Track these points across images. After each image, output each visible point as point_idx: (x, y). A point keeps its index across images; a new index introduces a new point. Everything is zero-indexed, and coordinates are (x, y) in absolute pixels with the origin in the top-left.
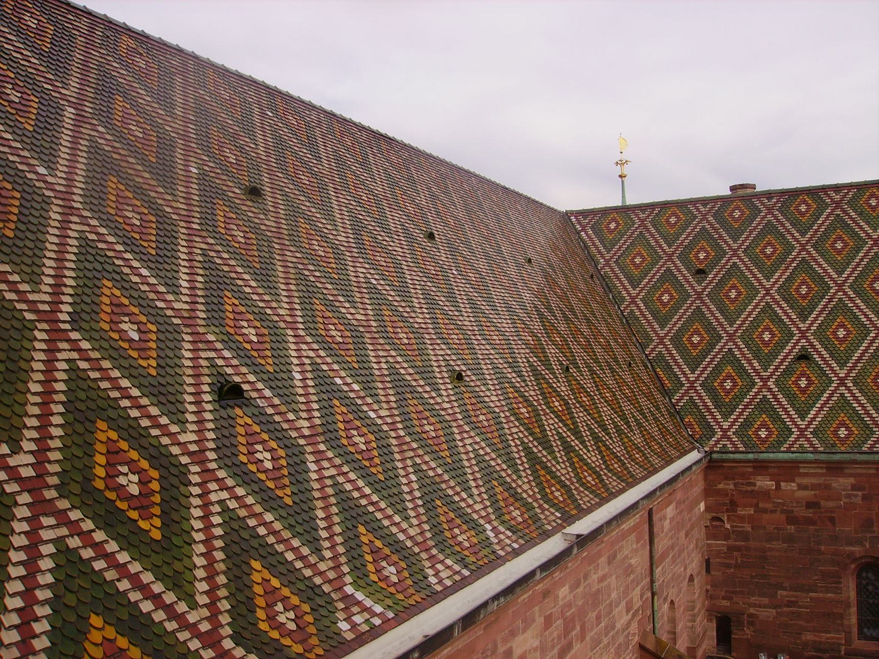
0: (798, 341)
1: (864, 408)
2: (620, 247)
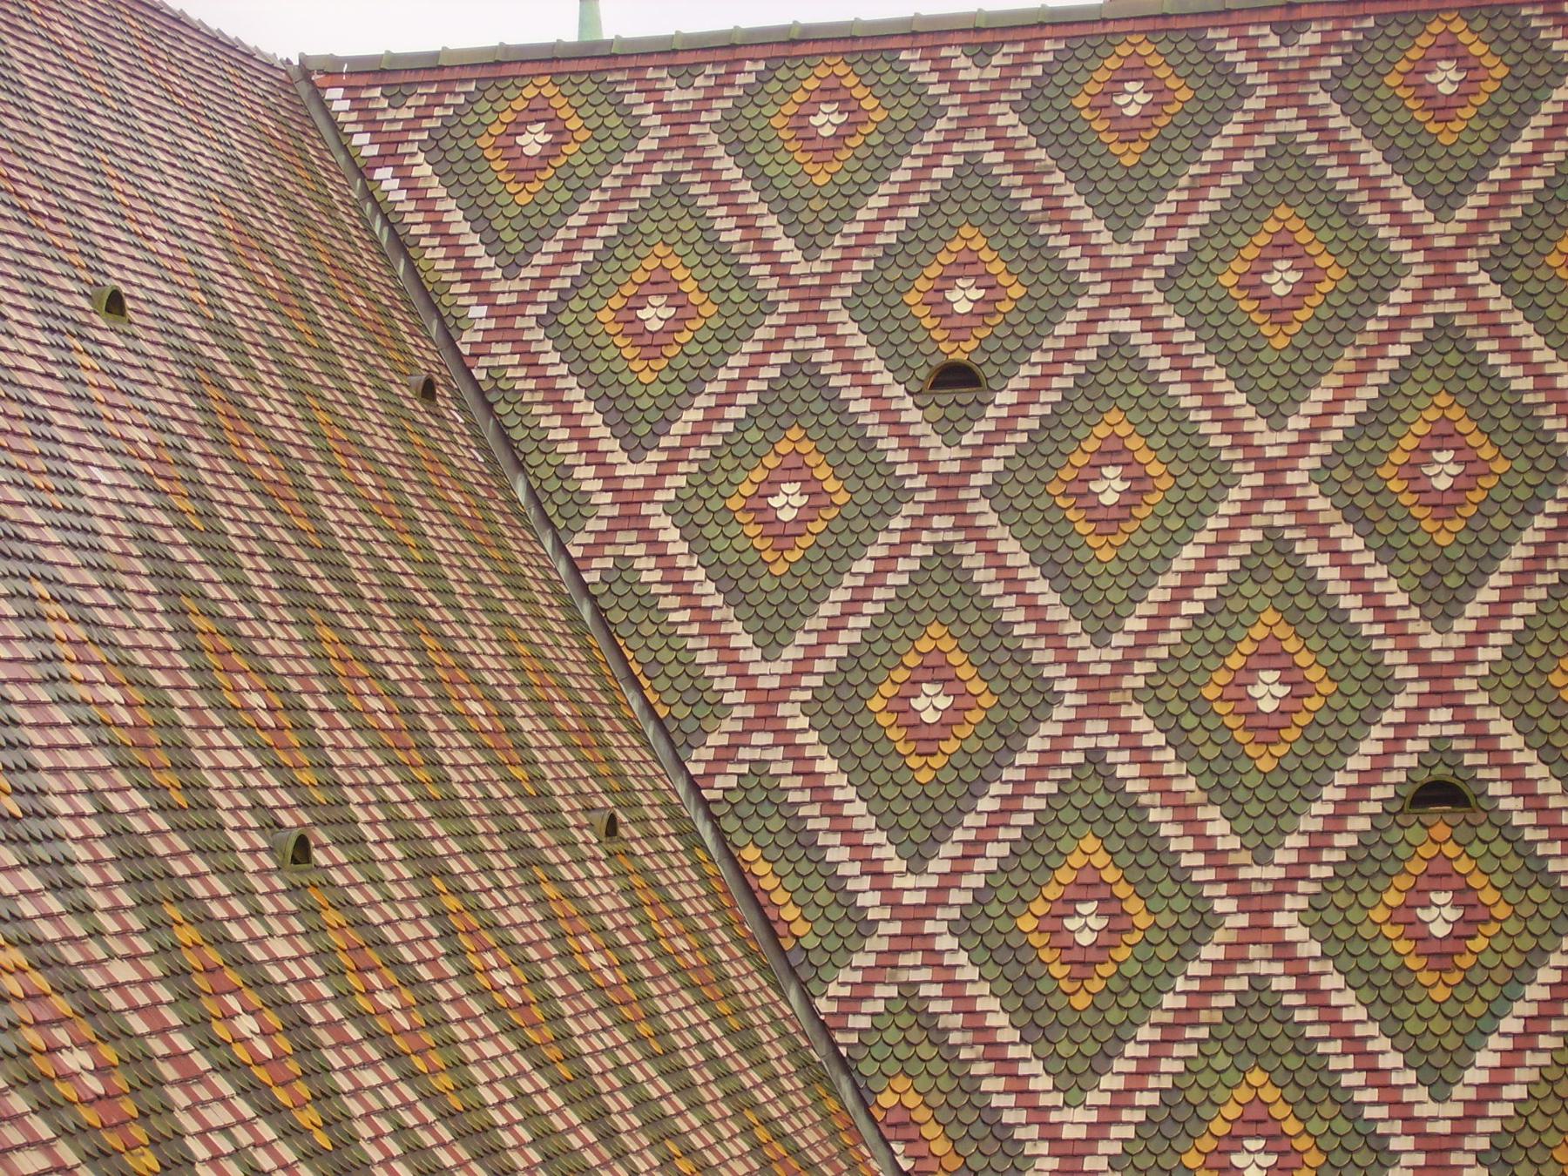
0: (1417, 715)
2: (570, 248)
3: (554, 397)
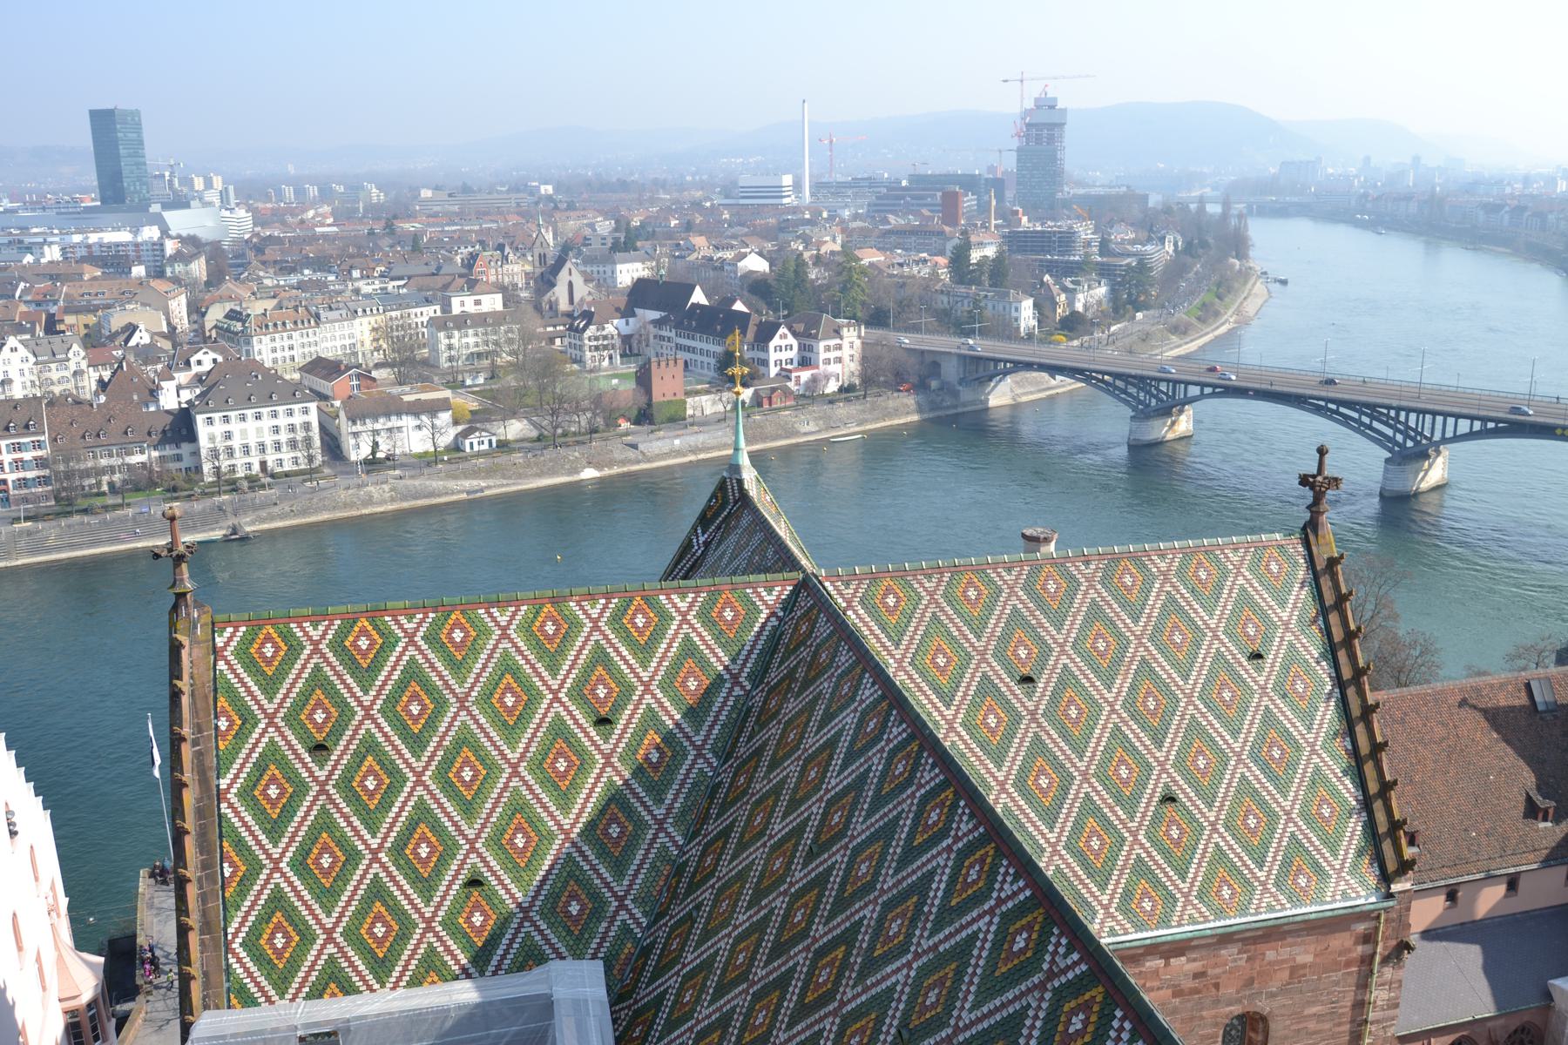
1: (1241, 858)
2: (912, 638)
3: (920, 689)
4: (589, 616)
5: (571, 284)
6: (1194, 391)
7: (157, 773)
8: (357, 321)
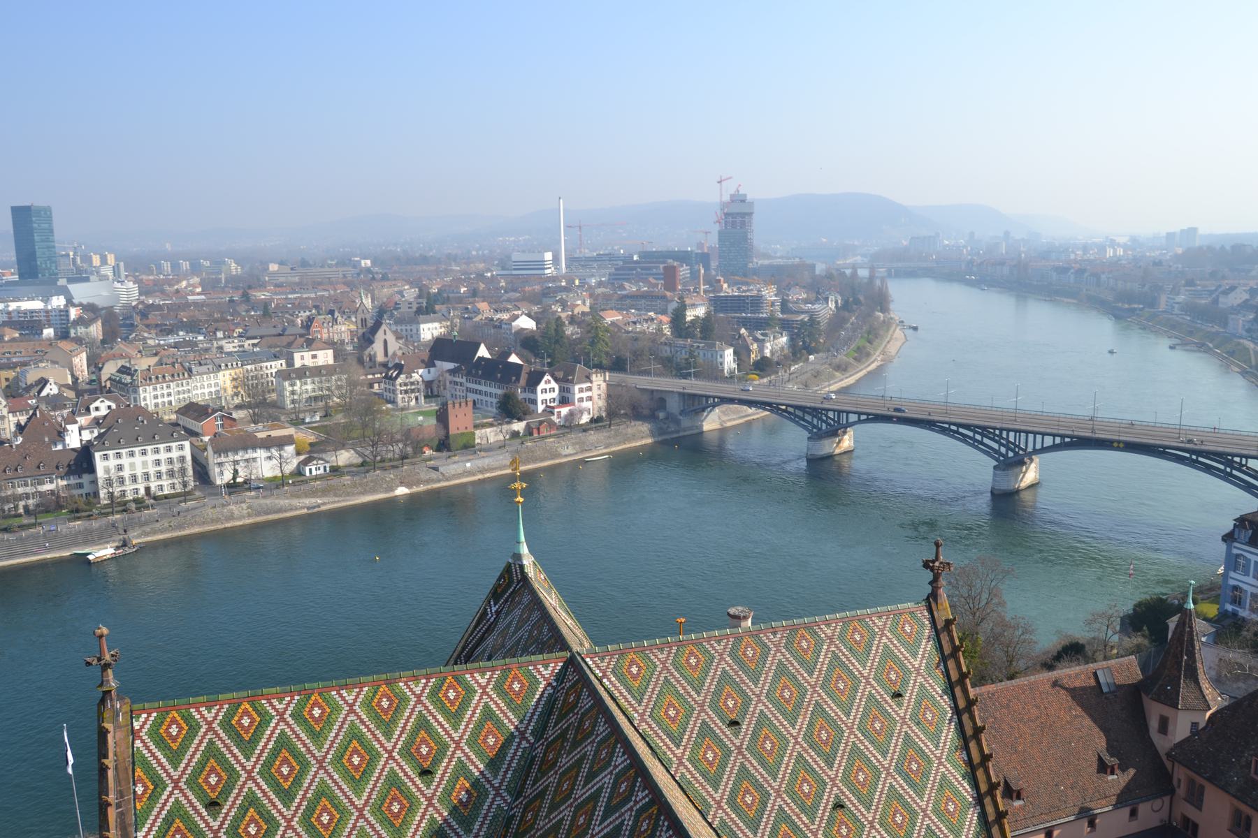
2: (650, 697)
3: (657, 735)
4: (413, 693)
5: (385, 342)
6: (853, 418)
7: (70, 771)
8: (221, 373)
